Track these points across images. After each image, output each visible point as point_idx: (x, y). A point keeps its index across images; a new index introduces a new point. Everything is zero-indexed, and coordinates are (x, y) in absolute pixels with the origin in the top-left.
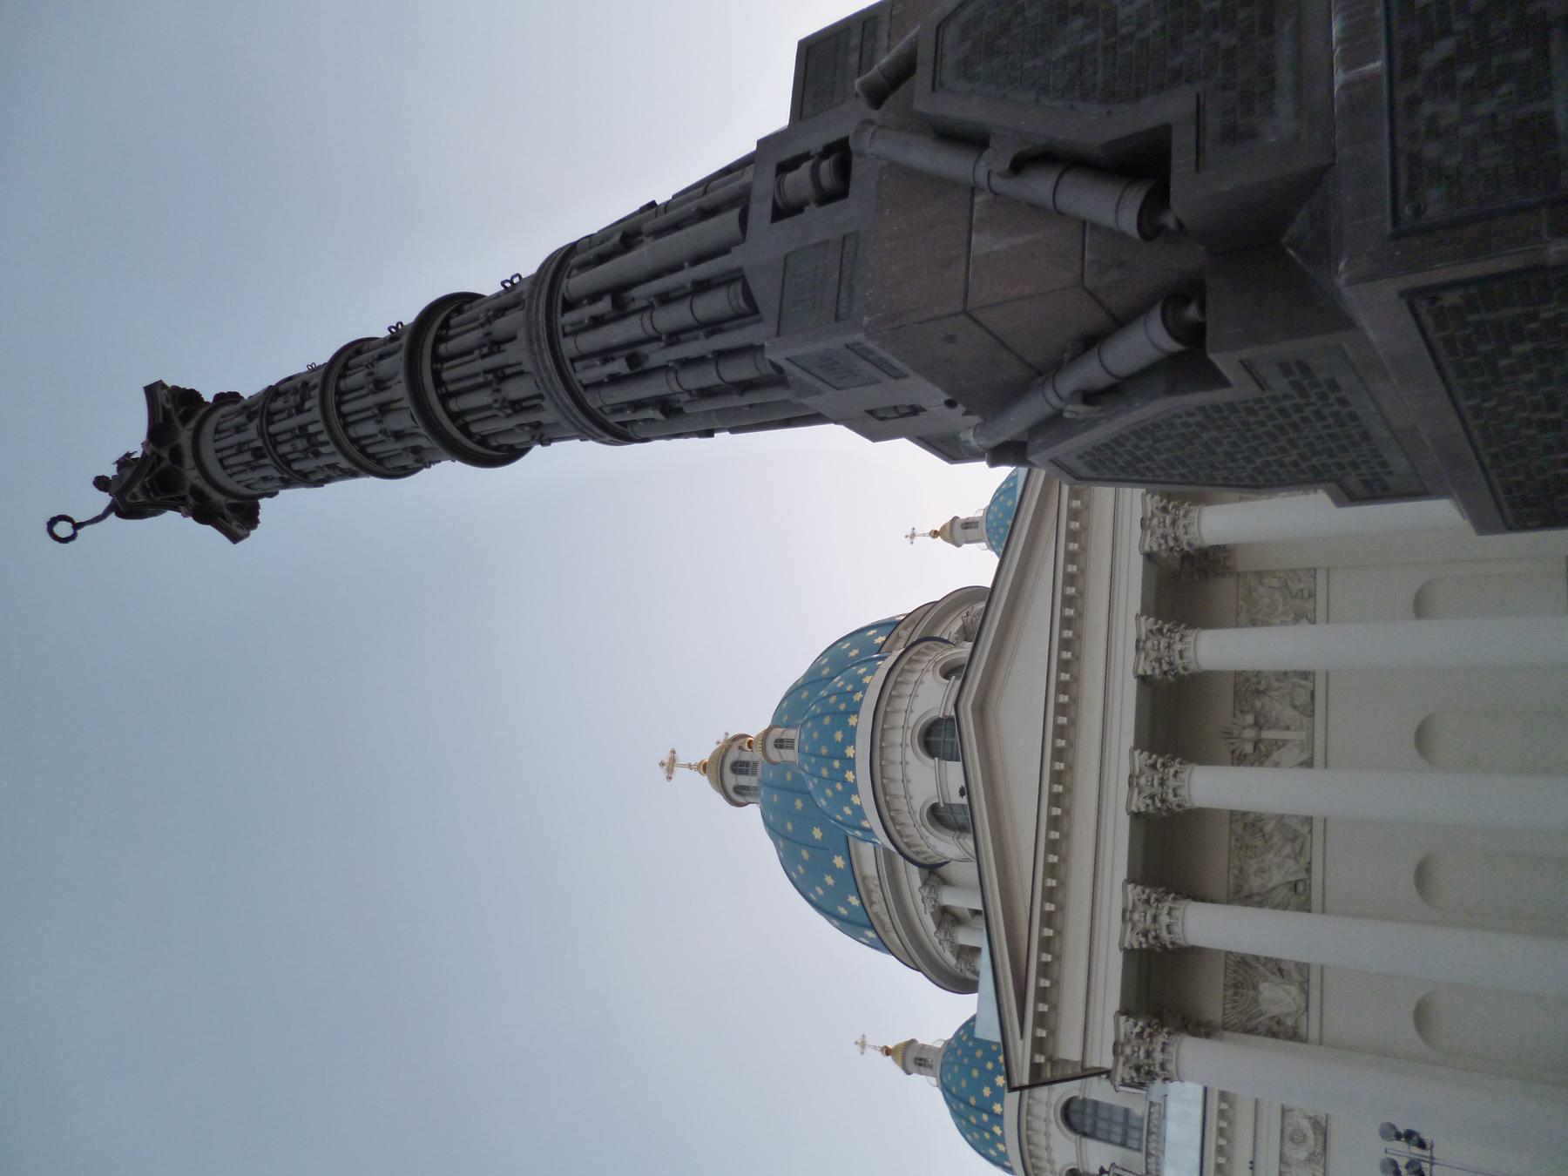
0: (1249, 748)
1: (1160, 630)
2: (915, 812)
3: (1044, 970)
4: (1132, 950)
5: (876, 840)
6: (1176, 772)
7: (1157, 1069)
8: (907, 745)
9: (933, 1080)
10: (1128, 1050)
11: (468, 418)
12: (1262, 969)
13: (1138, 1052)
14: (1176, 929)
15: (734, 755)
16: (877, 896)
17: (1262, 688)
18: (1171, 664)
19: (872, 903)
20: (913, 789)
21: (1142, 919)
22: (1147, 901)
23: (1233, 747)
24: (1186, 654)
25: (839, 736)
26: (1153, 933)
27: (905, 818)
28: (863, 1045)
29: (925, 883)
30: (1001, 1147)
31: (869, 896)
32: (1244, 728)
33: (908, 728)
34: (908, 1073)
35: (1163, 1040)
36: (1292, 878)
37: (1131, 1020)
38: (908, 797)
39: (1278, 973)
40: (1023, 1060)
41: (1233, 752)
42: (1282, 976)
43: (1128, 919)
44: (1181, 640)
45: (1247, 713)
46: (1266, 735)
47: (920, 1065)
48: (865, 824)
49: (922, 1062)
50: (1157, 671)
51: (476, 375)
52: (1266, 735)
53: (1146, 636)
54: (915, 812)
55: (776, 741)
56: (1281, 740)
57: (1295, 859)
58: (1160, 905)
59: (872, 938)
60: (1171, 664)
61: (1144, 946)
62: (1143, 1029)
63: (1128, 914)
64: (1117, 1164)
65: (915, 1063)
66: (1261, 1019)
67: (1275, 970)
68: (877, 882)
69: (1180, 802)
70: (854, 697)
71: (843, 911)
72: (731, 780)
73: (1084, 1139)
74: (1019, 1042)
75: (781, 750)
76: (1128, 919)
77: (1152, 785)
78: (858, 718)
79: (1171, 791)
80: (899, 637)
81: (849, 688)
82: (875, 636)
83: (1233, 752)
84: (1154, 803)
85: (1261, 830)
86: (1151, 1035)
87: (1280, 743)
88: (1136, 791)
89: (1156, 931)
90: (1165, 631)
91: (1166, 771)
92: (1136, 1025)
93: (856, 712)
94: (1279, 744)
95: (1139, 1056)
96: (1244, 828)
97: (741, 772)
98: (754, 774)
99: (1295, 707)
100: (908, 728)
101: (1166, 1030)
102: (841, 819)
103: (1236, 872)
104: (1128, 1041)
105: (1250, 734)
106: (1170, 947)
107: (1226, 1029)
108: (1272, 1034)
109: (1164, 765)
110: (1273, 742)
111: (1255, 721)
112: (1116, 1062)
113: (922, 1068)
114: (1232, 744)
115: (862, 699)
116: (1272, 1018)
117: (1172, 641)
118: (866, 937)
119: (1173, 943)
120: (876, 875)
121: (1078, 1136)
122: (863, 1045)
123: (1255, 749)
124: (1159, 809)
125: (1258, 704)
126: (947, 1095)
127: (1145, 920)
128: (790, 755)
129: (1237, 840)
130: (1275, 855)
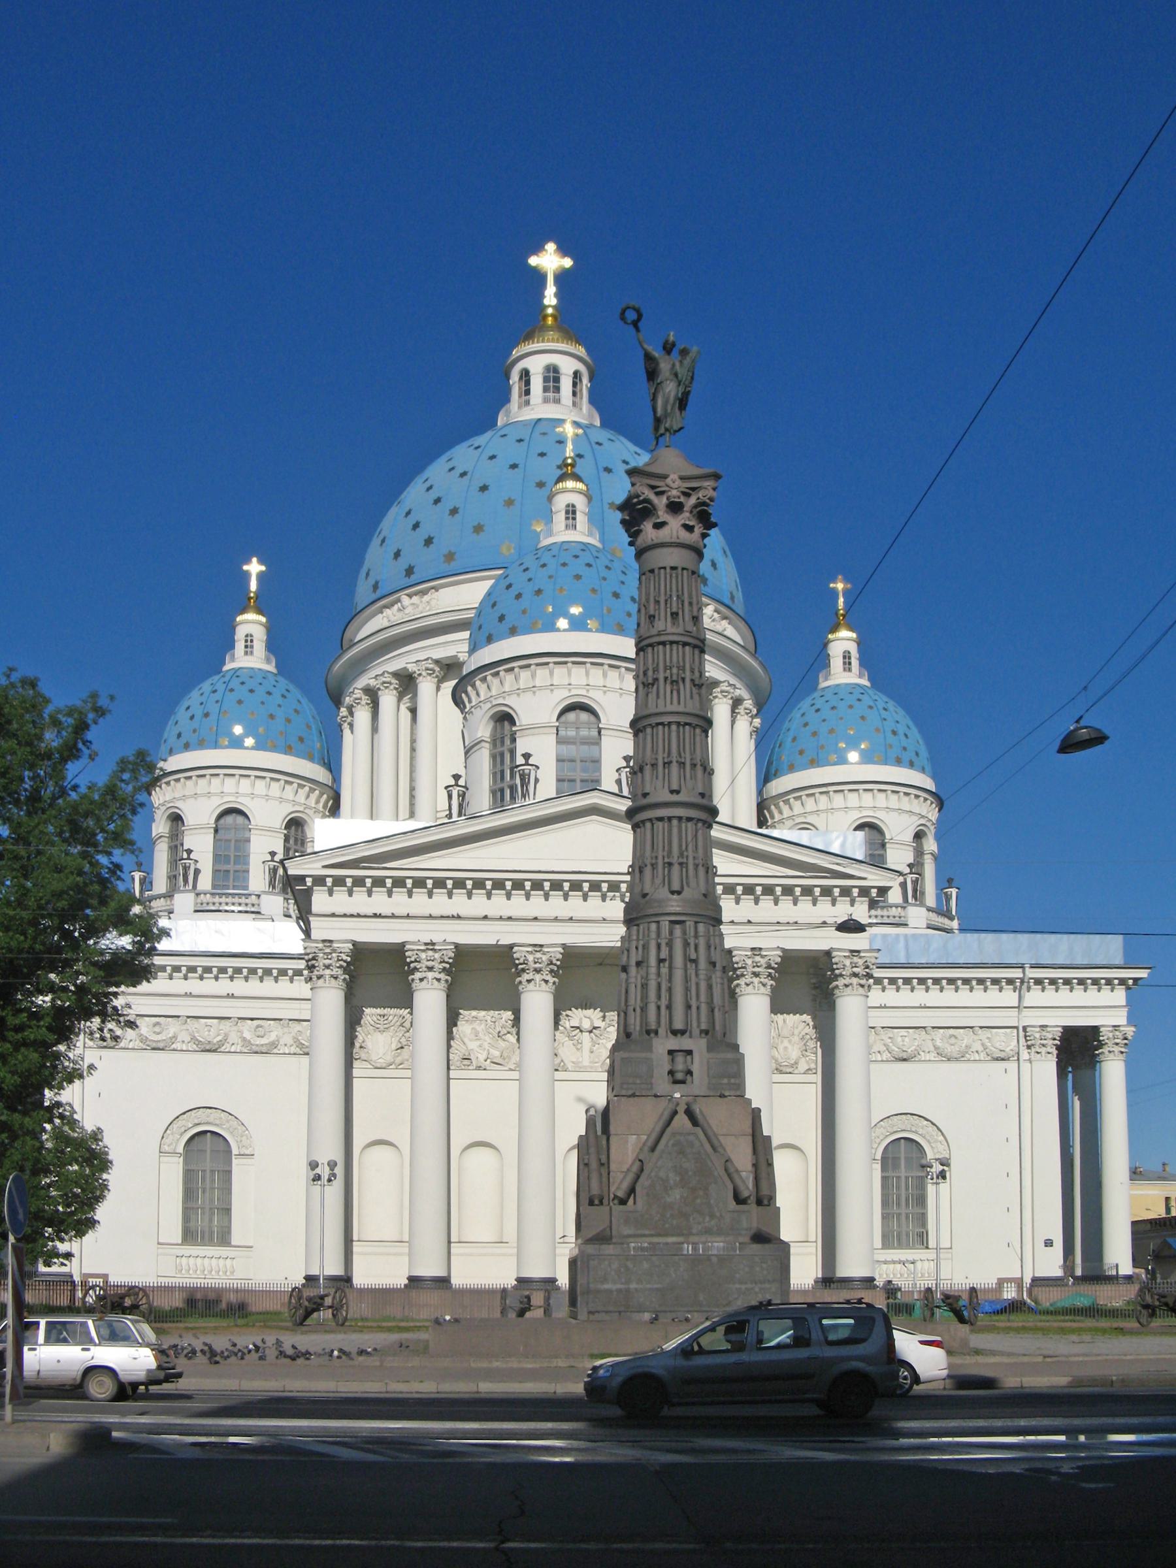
2: (504, 698)
8: (570, 690)
20: (529, 694)
29: (437, 662)
31: (416, 594)
33: (588, 691)
38: (518, 691)
54: (504, 698)
55: (573, 506)
61: (408, 960)
77: (535, 963)
98: (546, 401)
100: (588, 691)
112: (316, 941)
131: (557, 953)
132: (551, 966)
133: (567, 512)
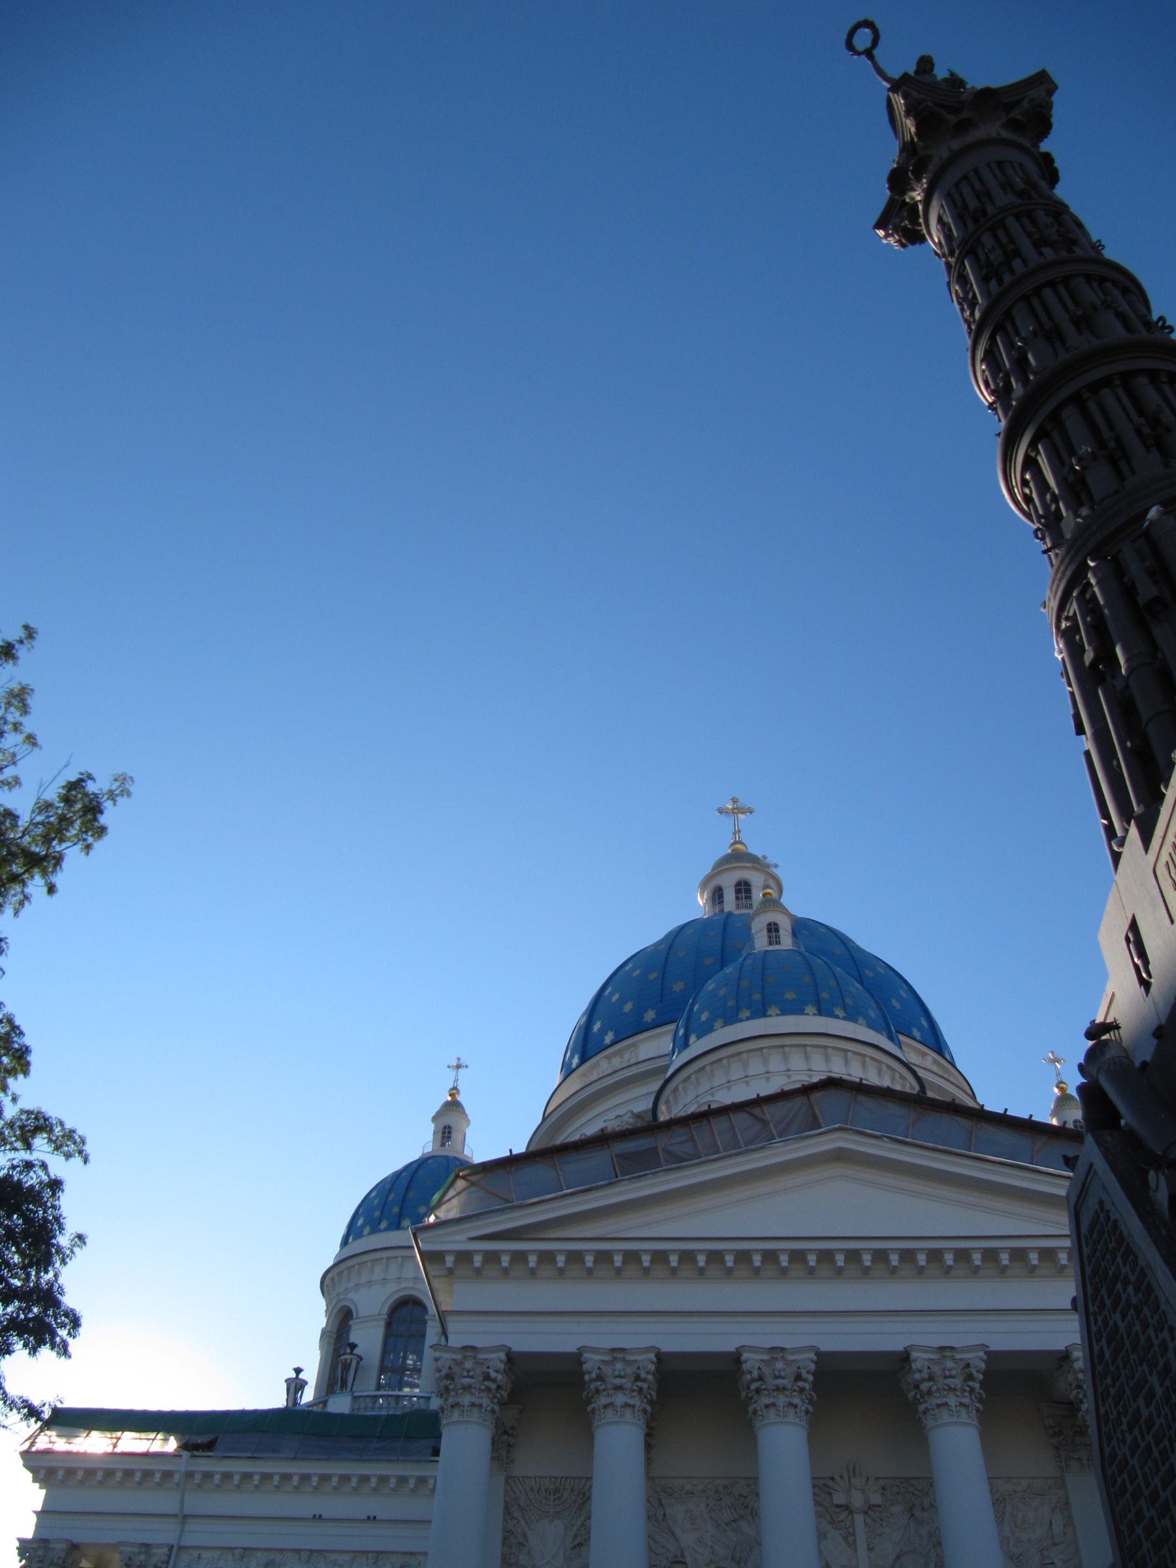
0: (839, 1498)
1: (970, 1377)
2: (712, 1095)
3: (547, 1257)
4: (581, 1363)
5: (676, 1053)
6: (795, 1406)
7: (451, 1401)
8: (789, 1077)
9: (429, 1149)
10: (469, 1364)
11: (1056, 435)
12: (579, 1523)
13: (468, 1376)
14: (609, 1414)
15: (756, 879)
16: (617, 1063)
17: (917, 1512)
18: (929, 1392)
19: (608, 1058)
21: (617, 1373)
22: (638, 1378)
23: (837, 1478)
24: (944, 1411)
25: (790, 996)
26: (602, 1388)
27: (705, 1086)
28: (458, 1067)
30: (367, 1230)
32: (863, 1491)
34: (434, 1119)
35: (484, 1405)
36: (688, 1559)
37: (502, 1366)
39: (576, 1543)
40: (451, 1242)
41: (832, 1479)
42: (574, 1548)
43: (615, 1355)
44: (962, 1404)
45: (883, 1495)
46: (859, 1519)
47: (444, 1133)
48: (693, 1038)
49: (446, 1135)
50: (917, 1376)
51: (1111, 427)
52: (859, 1519)
53: (961, 1360)
54: (712, 1095)
55: (775, 924)
56: (855, 1541)
57: (711, 1561)
58: (635, 1393)
59: (571, 1064)
60: (929, 1392)
61: (587, 1377)
62: (494, 1380)
63: (620, 1356)
64: (361, 1363)
65: (445, 1128)
66: (523, 1523)
67: (579, 1540)
68: (633, 1061)
69: (760, 1413)
70: (839, 1009)
71: (597, 1027)
72: (728, 883)
73: (383, 1323)
74: (464, 1237)
75: (765, 932)
76: (615, 1355)
77: (776, 1377)
78: (814, 1015)
79: (772, 1400)
80: (925, 1054)
81: (849, 1001)
82: (920, 1028)
83: (832, 1479)
84: (754, 1380)
85: (741, 1517)
86: (488, 1389)
87: (851, 1539)
88: (765, 1357)
89: (604, 1390)
90: (971, 1383)
91: (795, 1394)
92: (497, 1371)
93: (820, 1013)
94: (849, 1537)
95: (464, 1377)
96: (740, 1495)
97: (738, 891)
98: (738, 906)
99: (898, 1557)
100: (810, 1076)
101: (497, 1408)
102: (695, 1009)
103: (688, 1487)
104: (479, 1363)
105: (857, 1500)
106: (589, 1408)
107: (507, 1479)
108: (507, 1535)
109: (802, 1390)
110: (851, 1530)
111: (875, 1506)
113: (440, 1135)
114: (842, 1477)
115: (837, 1017)
116: (524, 1535)
117: (958, 1393)
118: (572, 1057)
119: (593, 1411)
120: (641, 1059)
121: (386, 1317)
122: (458, 1067)
123: (838, 1506)
124: (748, 1388)
125: (896, 1509)
126: (415, 1166)
127: (616, 1377)
128: (761, 943)
129: (725, 1487)
130: (713, 1536)
131: (807, 1362)
132: (800, 1384)
133: (769, 931)
